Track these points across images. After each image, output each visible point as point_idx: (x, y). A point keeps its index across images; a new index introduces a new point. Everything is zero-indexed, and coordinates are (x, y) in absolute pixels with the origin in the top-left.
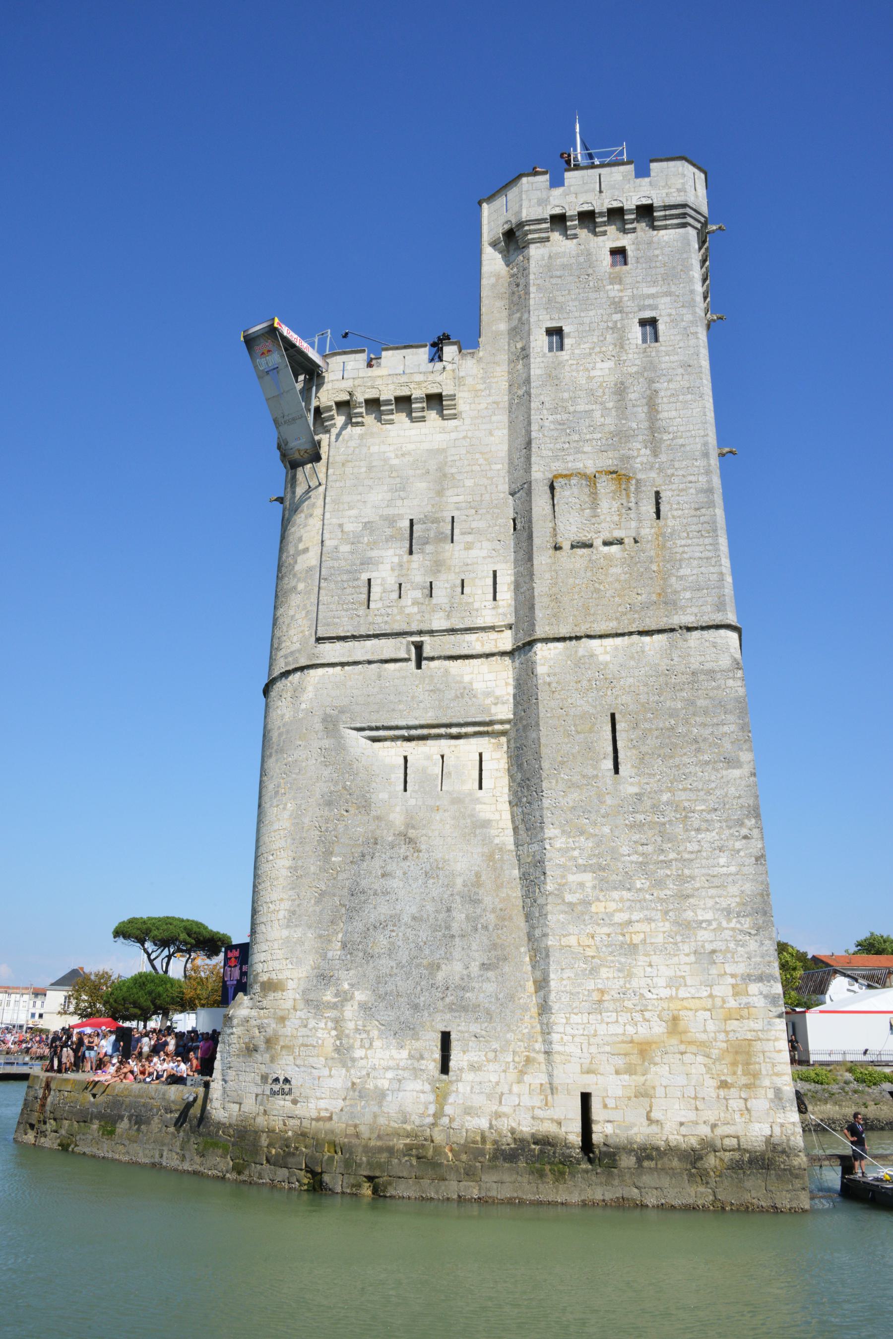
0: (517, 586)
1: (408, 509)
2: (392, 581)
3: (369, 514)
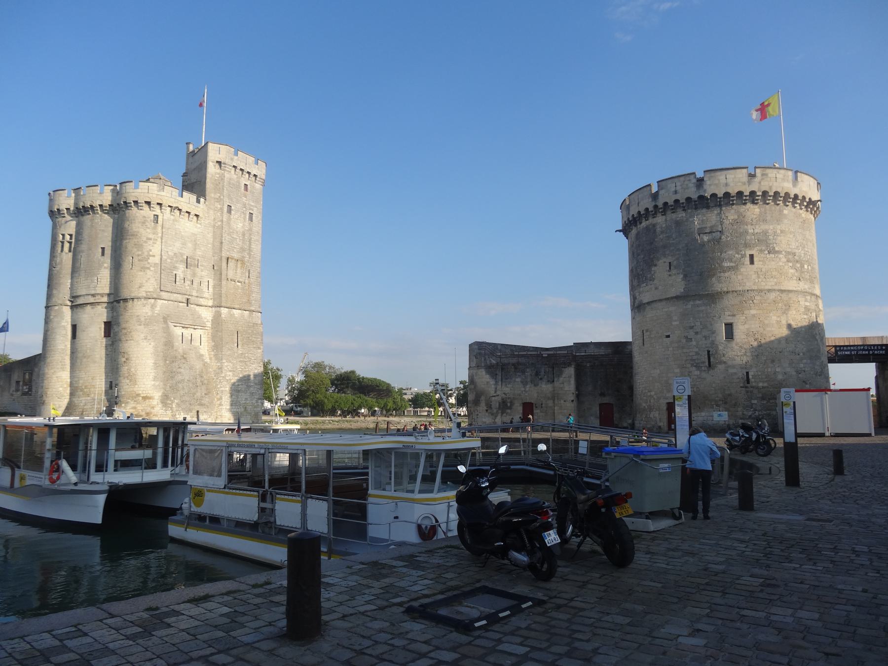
0: (214, 287)
1: (187, 252)
2: (182, 276)
3: (176, 250)
